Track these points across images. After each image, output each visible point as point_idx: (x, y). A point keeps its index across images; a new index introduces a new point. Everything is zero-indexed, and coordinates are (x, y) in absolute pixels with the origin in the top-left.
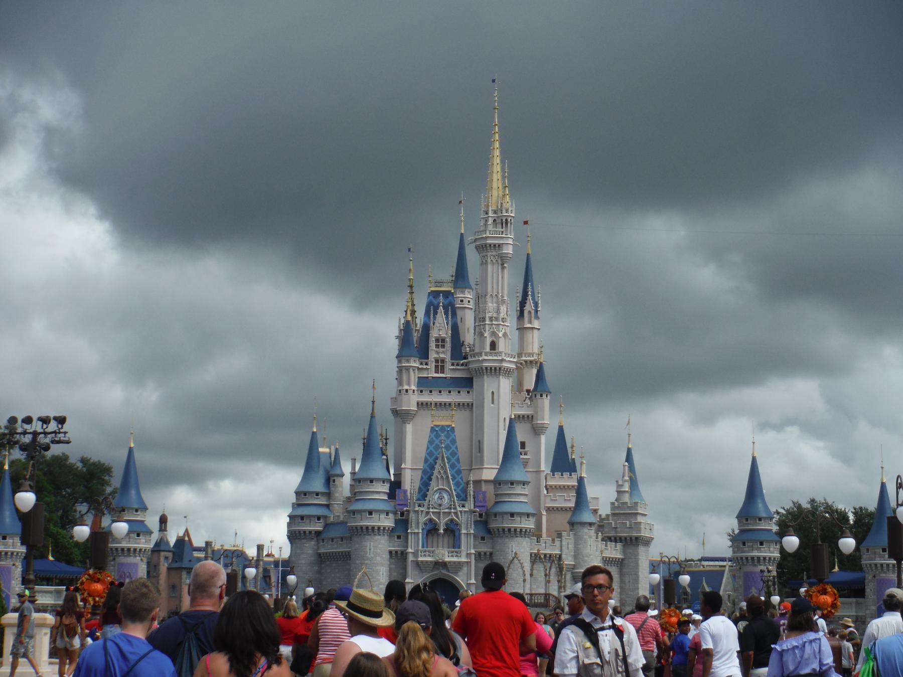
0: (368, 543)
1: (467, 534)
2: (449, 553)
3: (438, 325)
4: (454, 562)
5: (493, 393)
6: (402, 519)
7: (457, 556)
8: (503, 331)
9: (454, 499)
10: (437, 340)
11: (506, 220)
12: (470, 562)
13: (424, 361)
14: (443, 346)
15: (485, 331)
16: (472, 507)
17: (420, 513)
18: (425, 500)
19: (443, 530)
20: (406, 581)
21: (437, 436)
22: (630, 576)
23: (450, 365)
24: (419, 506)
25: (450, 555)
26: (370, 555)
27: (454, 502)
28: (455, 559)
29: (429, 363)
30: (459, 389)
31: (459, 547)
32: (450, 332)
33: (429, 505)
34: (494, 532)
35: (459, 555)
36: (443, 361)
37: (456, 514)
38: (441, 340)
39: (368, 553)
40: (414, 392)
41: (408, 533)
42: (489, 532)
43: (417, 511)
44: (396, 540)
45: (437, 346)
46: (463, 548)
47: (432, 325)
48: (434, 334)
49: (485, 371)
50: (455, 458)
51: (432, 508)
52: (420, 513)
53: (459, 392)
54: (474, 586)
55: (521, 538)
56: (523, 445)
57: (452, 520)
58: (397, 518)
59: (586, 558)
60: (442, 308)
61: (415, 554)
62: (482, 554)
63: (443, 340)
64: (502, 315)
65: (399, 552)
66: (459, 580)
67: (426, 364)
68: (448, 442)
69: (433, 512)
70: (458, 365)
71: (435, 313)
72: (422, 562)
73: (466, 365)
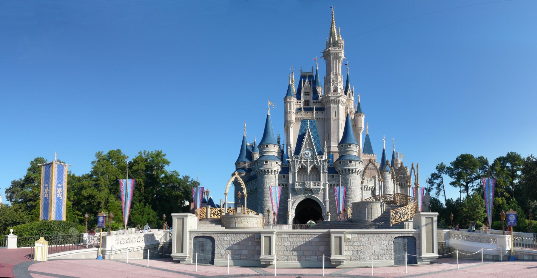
1: (324, 173)
2: (313, 183)
4: (316, 189)
6: (286, 167)
7: (318, 185)
9: (316, 154)
12: (326, 189)
13: (299, 101)
14: (309, 95)
16: (326, 158)
17: (296, 162)
18: (299, 155)
19: (310, 171)
20: (288, 200)
21: (306, 124)
23: (312, 102)
24: (296, 158)
25: (314, 185)
26: (267, 185)
27: (316, 155)
28: (317, 187)
31: (319, 180)
33: (301, 157)
34: (340, 172)
35: (319, 185)
36: (309, 101)
37: (317, 162)
40: (293, 112)
41: (289, 174)
42: (337, 173)
43: (295, 161)
44: (282, 178)
46: (321, 181)
50: (316, 134)
51: (303, 159)
52: (296, 162)
54: (329, 201)
55: (355, 175)
57: (315, 166)
58: (283, 167)
59: (388, 189)
61: (293, 184)
62: (333, 185)
65: (284, 185)
66: (320, 199)
67: (300, 102)
68: (312, 127)
69: (303, 161)
70: (316, 102)
71: (304, 82)
72: (297, 189)
73: (321, 102)
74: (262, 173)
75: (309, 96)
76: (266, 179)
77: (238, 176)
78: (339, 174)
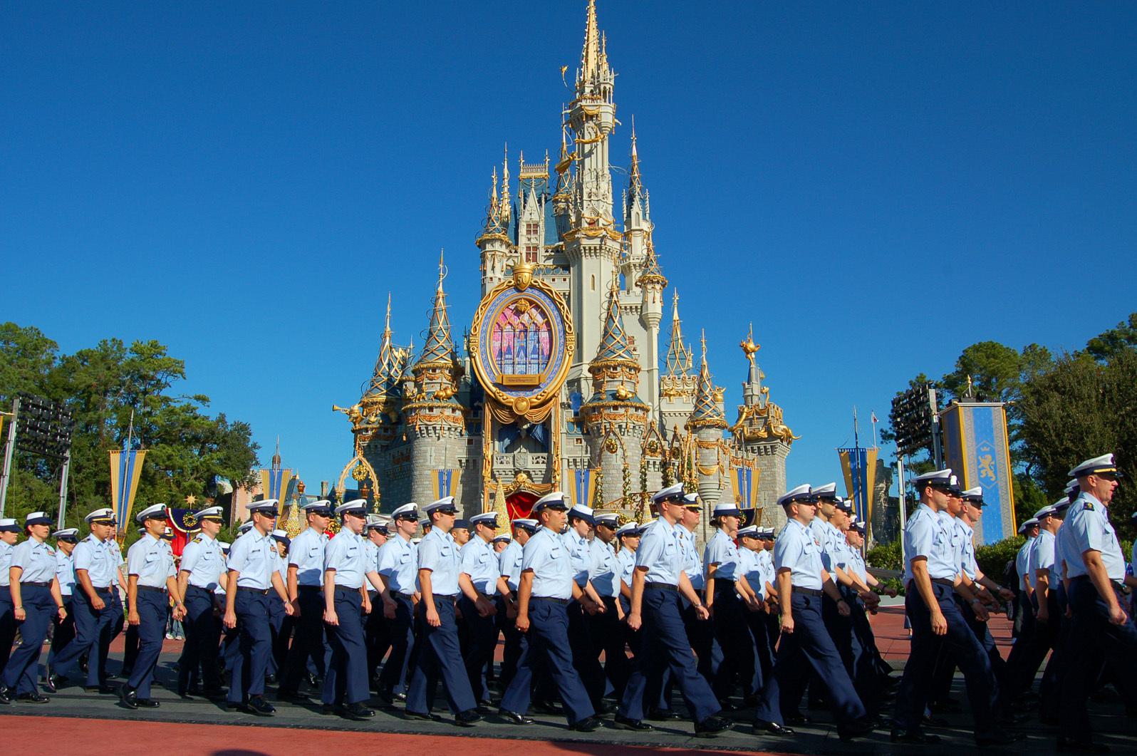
0: (429, 448)
3: (530, 209)
5: (593, 276)
8: (604, 208)
10: (529, 226)
11: (605, 88)
15: (583, 209)
22: (766, 492)
25: (535, 461)
29: (519, 251)
30: (553, 276)
32: (543, 215)
36: (536, 248)
38: (534, 225)
39: (429, 461)
45: (529, 232)
47: (522, 208)
48: (525, 219)
49: (583, 251)
53: (554, 280)
56: (632, 340)
60: (533, 189)
63: (536, 225)
64: (602, 191)
67: (516, 252)
74: (421, 434)
75: (536, 236)
76: (429, 448)
77: (363, 458)
78: (592, 436)
